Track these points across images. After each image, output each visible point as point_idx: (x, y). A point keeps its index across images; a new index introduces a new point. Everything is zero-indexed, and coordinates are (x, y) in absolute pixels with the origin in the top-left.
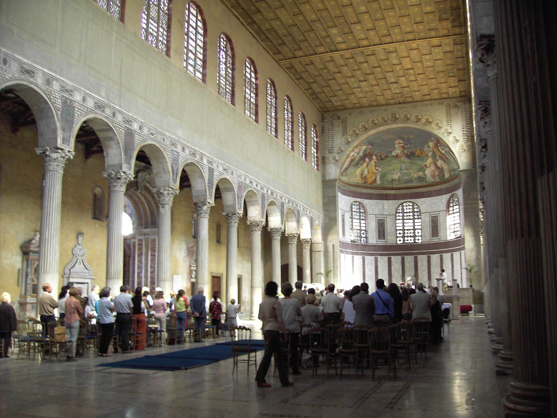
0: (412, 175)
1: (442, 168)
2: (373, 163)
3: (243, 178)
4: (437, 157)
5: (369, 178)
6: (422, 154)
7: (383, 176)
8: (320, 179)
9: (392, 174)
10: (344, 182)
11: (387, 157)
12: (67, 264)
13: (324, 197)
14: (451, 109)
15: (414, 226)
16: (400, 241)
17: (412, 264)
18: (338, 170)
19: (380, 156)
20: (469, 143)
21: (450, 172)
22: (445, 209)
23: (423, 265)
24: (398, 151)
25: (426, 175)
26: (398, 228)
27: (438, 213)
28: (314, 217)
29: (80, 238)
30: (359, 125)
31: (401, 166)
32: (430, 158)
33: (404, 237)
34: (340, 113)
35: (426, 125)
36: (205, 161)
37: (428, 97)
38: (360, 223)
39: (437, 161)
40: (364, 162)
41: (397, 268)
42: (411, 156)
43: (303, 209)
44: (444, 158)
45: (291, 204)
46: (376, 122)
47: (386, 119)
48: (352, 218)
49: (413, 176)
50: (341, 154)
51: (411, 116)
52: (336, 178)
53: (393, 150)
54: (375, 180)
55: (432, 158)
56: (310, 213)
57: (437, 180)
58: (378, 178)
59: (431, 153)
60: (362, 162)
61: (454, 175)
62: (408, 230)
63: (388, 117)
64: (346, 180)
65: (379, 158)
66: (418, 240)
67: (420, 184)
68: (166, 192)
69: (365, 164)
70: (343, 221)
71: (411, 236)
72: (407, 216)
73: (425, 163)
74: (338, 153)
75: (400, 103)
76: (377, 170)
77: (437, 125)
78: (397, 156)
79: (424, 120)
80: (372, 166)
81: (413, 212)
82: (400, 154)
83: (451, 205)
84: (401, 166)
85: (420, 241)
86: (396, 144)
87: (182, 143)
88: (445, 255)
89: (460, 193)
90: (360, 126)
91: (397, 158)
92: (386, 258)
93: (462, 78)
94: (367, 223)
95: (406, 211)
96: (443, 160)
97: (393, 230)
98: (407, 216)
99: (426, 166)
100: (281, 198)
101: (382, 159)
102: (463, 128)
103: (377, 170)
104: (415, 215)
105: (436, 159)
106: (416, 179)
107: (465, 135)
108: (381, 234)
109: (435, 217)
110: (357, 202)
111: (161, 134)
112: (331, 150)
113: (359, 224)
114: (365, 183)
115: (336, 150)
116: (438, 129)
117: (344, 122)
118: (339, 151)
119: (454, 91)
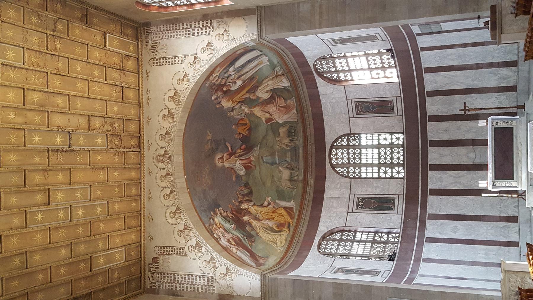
0: (284, 146)
1: (271, 90)
2: (253, 209)
5: (282, 220)
6: (246, 124)
7: (281, 196)
9: (279, 180)
10: (278, 263)
11: (246, 185)
15: (372, 147)
16: (400, 173)
17: (446, 150)
18: (243, 271)
20: (214, 23)
21: (277, 76)
23: (446, 131)
24: (238, 165)
25: (285, 123)
26: (376, 176)
27: (349, 101)
31: (267, 163)
32: (253, 110)
33: (392, 166)
34: (149, 259)
35: (179, 101)
37: (130, 94)
38: (360, 241)
39: (258, 98)
40: (250, 224)
46: (168, 191)
47: (164, 173)
48: (348, 256)
49: (287, 145)
52: (258, 277)
53: (236, 172)
54: (288, 210)
55: (254, 107)
57: (292, 102)
58: (283, 204)
59: (243, 107)
60: (247, 228)
61: (281, 67)
62: (380, 158)
64: (275, 258)
65: (247, 198)
66: (398, 139)
67: (301, 134)
69: (254, 223)
70: (348, 271)
71: (392, 153)
72: (355, 159)
73: (264, 120)
74: (215, 267)
75: (139, 146)
76: (269, 204)
77: (180, 81)
79: (172, 105)
80: (261, 213)
81: (348, 147)
82: (244, 162)
83: (335, 75)
84: (267, 163)
85: (401, 136)
86: (224, 166)
88: (428, 87)
92: (431, 199)
93: (78, 14)
94: (360, 229)
95: (345, 161)
96: (255, 88)
97: (379, 183)
98: (355, 159)
99: (268, 120)
101: (251, 193)
102: (189, 34)
103: (269, 204)
104: (354, 145)
105: (255, 99)
106: (291, 140)
107: (200, 31)
108: (385, 204)
109: (357, 107)
110: (320, 245)
112: (208, 281)
113: (362, 245)
114: (289, 227)
115: (208, 271)
117: (163, 251)
118: (212, 265)
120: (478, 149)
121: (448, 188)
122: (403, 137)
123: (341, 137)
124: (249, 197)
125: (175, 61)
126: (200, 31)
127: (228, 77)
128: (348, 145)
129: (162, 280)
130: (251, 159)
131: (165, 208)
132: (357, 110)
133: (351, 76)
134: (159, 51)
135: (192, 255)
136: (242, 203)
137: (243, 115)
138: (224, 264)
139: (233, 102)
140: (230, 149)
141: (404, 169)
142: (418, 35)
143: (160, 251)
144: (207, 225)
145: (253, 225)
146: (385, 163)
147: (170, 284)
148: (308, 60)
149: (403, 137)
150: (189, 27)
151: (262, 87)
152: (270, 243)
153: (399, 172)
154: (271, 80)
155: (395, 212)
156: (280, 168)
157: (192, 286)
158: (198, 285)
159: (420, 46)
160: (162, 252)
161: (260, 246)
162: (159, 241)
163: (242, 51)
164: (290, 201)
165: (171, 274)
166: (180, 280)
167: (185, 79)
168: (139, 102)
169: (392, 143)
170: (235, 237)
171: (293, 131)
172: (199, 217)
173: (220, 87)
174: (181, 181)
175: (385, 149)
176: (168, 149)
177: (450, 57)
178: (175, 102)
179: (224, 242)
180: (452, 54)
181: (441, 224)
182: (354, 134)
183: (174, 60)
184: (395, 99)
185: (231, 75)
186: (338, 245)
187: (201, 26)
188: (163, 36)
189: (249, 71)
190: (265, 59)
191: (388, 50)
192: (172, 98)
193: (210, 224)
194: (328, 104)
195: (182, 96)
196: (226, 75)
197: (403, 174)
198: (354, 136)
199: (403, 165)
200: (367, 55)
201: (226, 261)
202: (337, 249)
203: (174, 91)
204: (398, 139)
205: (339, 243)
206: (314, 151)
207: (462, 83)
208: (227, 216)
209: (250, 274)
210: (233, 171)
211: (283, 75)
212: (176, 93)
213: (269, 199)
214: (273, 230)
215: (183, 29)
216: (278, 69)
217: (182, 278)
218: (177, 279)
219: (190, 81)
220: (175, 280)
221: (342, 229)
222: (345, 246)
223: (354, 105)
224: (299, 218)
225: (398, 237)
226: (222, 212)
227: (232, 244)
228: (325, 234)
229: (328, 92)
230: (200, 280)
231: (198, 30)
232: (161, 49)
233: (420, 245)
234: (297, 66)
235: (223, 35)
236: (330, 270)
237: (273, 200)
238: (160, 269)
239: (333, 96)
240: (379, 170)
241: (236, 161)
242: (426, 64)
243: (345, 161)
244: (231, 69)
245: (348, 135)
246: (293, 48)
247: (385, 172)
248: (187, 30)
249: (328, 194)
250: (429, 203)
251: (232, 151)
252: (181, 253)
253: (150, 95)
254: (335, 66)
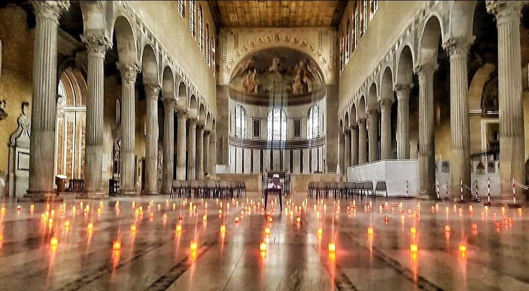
3: (178, 69)
4: (304, 75)
7: (260, 87)
11: (264, 71)
12: (13, 133)
13: (217, 99)
19: (260, 71)
29: (25, 107)
34: (233, 30)
36: (157, 46)
39: (303, 77)
42: (283, 72)
44: (310, 76)
58: (256, 87)
68: (131, 69)
69: (248, 76)
78: (272, 72)
79: (301, 42)
87: (143, 24)
89: (323, 103)
99: (294, 81)
100: (198, 93)
108: (256, 133)
111: (130, 9)
115: (228, 59)
119: (328, 20)
139: (302, 67)
192: (303, 43)
201: (233, 69)
253: (305, 31)
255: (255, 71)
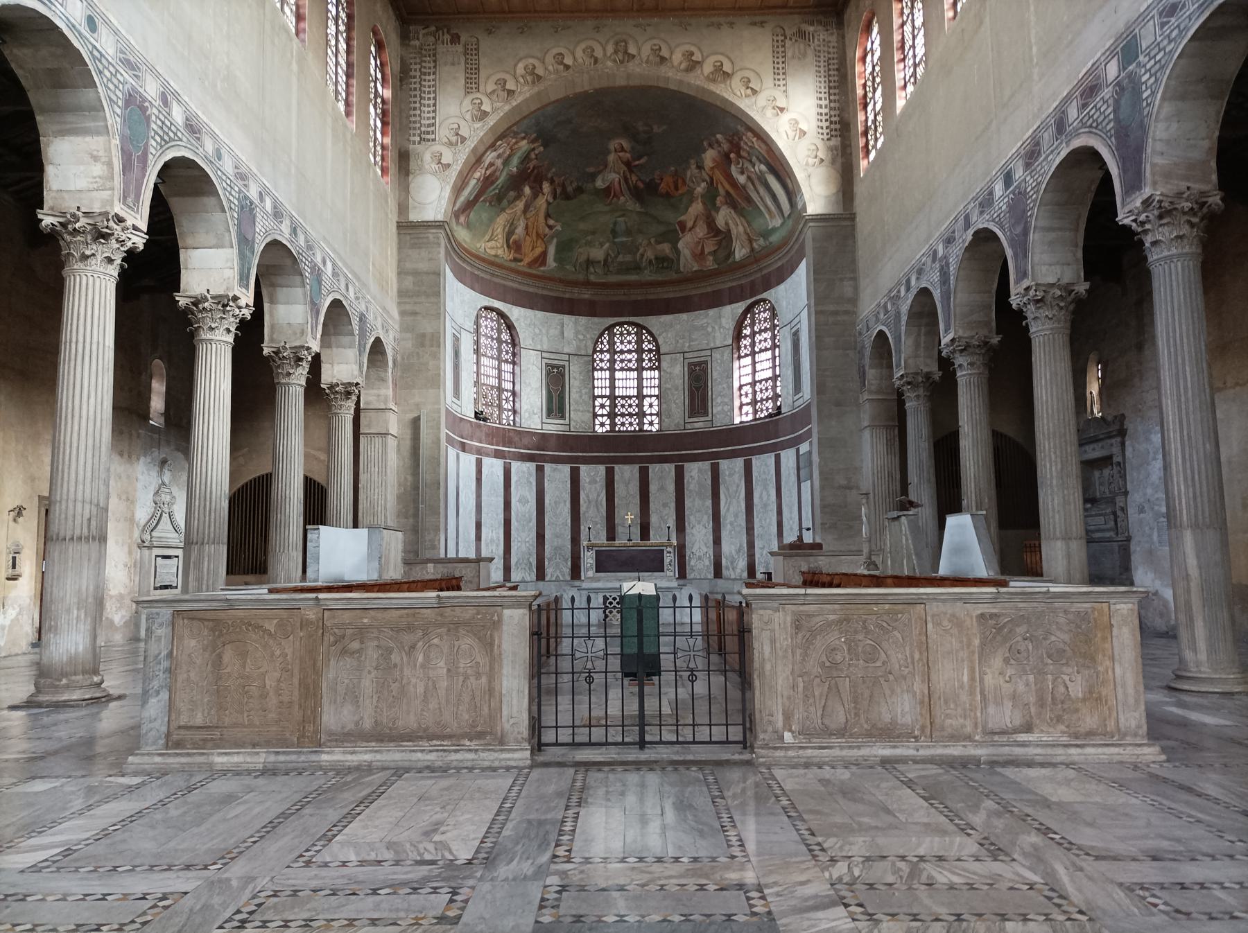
0: (641, 250)
1: (729, 231)
2: (541, 202)
4: (719, 200)
5: (526, 248)
6: (677, 188)
7: (564, 248)
8: (393, 218)
9: (589, 244)
10: (459, 244)
11: (579, 190)
13: (401, 273)
14: (788, 43)
15: (640, 387)
16: (602, 427)
17: (634, 488)
19: (563, 186)
20: (836, 142)
21: (750, 241)
22: (730, 341)
23: (662, 488)
25: (678, 252)
26: (597, 392)
27: (708, 353)
28: (370, 317)
30: (515, 66)
33: (612, 415)
35: (714, 81)
39: (717, 210)
40: (518, 197)
41: (593, 496)
42: (646, 192)
43: (335, 274)
44: (741, 202)
45: (285, 228)
47: (599, 53)
48: (477, 352)
49: (642, 255)
50: (460, 146)
51: (672, 53)
52: (440, 217)
53: (600, 172)
55: (704, 204)
56: (357, 298)
57: (710, 264)
58: (552, 250)
60: (512, 194)
61: (763, 248)
62: (623, 397)
63: (604, 50)
64: (467, 239)
65: (558, 191)
67: (659, 278)
69: (520, 205)
70: (456, 354)
71: (631, 415)
72: (622, 361)
73: (682, 218)
74: (450, 144)
76: (550, 227)
77: (747, 82)
78: (607, 191)
79: (708, 68)
81: (640, 351)
82: (616, 184)
83: (747, 331)
84: (615, 224)
85: (655, 428)
86: (609, 152)
88: (724, 464)
90: (520, 69)
91: (608, 196)
92: (566, 469)
95: (619, 347)
96: (733, 205)
97: (586, 397)
98: (622, 361)
101: (567, 197)
102: (821, 99)
103: (550, 227)
104: (643, 360)
105: (714, 204)
106: (650, 262)
107: (824, 118)
109: (700, 364)
110: (492, 309)
112: (428, 133)
113: (495, 373)
114: (515, 260)
115: (443, 133)
116: (747, 96)
118: (454, 139)
120: (636, 531)
121: (581, 492)
122: (654, 430)
123: (655, 340)
124: (561, 194)
125: (778, 74)
126: (824, 118)
127: (751, 161)
128: (643, 351)
129: (423, 52)
130: (622, 198)
131: (539, 55)
132: (695, 364)
133: (746, 355)
134: (796, 45)
135: (467, 101)
136: (551, 184)
137: (691, 185)
138: (455, 161)
139: (712, 168)
140: (637, 163)
141: (607, 431)
142: (798, 450)
143: (470, 47)
144: (515, 128)
145: (517, 202)
146: (616, 406)
147: (418, 66)
148: (772, 291)
149: (654, 430)
150: (832, 97)
151: (735, 216)
152: (490, 231)
153: (602, 425)
154: (745, 230)
155: (545, 420)
156: (607, 245)
157: (418, 105)
158: (420, 115)
159: (783, 454)
160: (469, 52)
161: (485, 216)
162: (486, 44)
163: (790, 185)
164: (555, 260)
165: (435, 67)
166: (427, 83)
167: (749, 91)
168: (714, 9)
169: (644, 415)
170: (498, 173)
171: (665, 264)
172: (528, 115)
173: (736, 148)
174: (584, 84)
175: (637, 406)
176: (637, 61)
177: (764, 493)
178: (712, 73)
179: (490, 157)
180: (769, 495)
181: (531, 483)
182: (658, 360)
183: (781, 71)
184: (709, 418)
185: (754, 166)
186: (492, 337)
187: (833, 119)
188: (819, 51)
189: (759, 196)
190: (777, 222)
191: (779, 408)
192: (719, 69)
193: (516, 134)
194: (705, 321)
195: (723, 85)
196: (754, 159)
197: (600, 431)
198: (656, 360)
199: (612, 430)
200: (774, 378)
202: (486, 335)
203: (730, 72)
204: (651, 423)
205: (496, 339)
206: (633, 298)
207: (728, 509)
208: (531, 160)
209: (444, 202)
210: (601, 167)
211: (752, 249)
212: (728, 74)
213: (559, 228)
214: (509, 234)
215: (830, 88)
216: (761, 241)
217: (429, 86)
218: (427, 78)
219: (747, 100)
220: (425, 74)
221: (517, 341)
222: (492, 347)
223: (702, 359)
224: (530, 275)
225: (509, 425)
226: (537, 152)
227: (487, 169)
228: (508, 318)
229: (724, 321)
230: (428, 118)
231: (826, 114)
232: (799, 48)
233: (498, 455)
234: (765, 272)
235: (816, 157)
236: (457, 327)
237: (557, 234)
238: (441, 49)
239: (717, 328)
240: (605, 396)
241: (619, 174)
242: (757, 461)
243: (619, 347)
244: (763, 167)
245: (658, 350)
246: (790, 269)
247: (602, 406)
248: (827, 95)
249: (568, 320)
250: (560, 466)
251: (636, 166)
252: (469, 85)
254: (761, 331)
255: (546, 187)
